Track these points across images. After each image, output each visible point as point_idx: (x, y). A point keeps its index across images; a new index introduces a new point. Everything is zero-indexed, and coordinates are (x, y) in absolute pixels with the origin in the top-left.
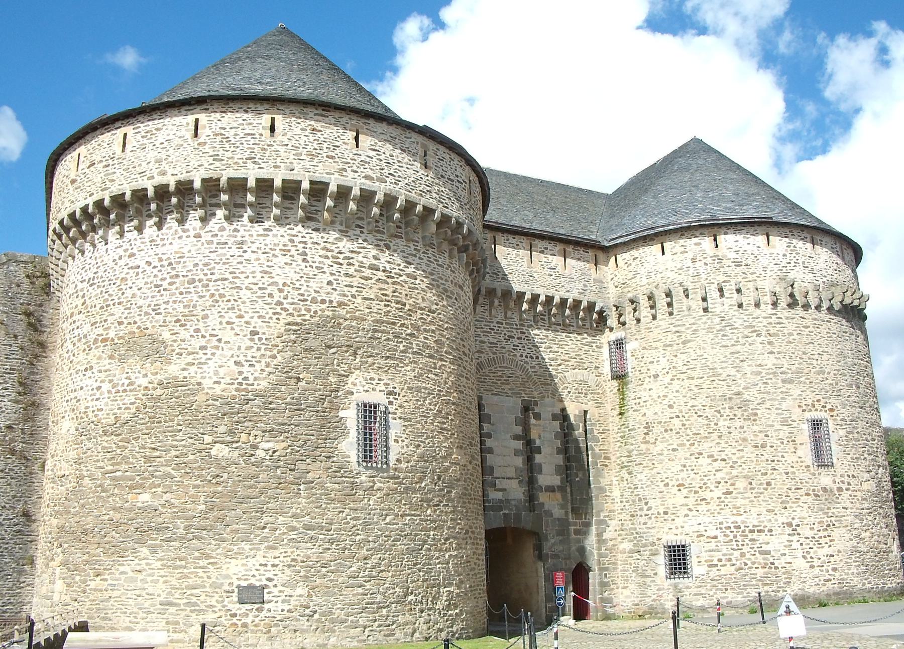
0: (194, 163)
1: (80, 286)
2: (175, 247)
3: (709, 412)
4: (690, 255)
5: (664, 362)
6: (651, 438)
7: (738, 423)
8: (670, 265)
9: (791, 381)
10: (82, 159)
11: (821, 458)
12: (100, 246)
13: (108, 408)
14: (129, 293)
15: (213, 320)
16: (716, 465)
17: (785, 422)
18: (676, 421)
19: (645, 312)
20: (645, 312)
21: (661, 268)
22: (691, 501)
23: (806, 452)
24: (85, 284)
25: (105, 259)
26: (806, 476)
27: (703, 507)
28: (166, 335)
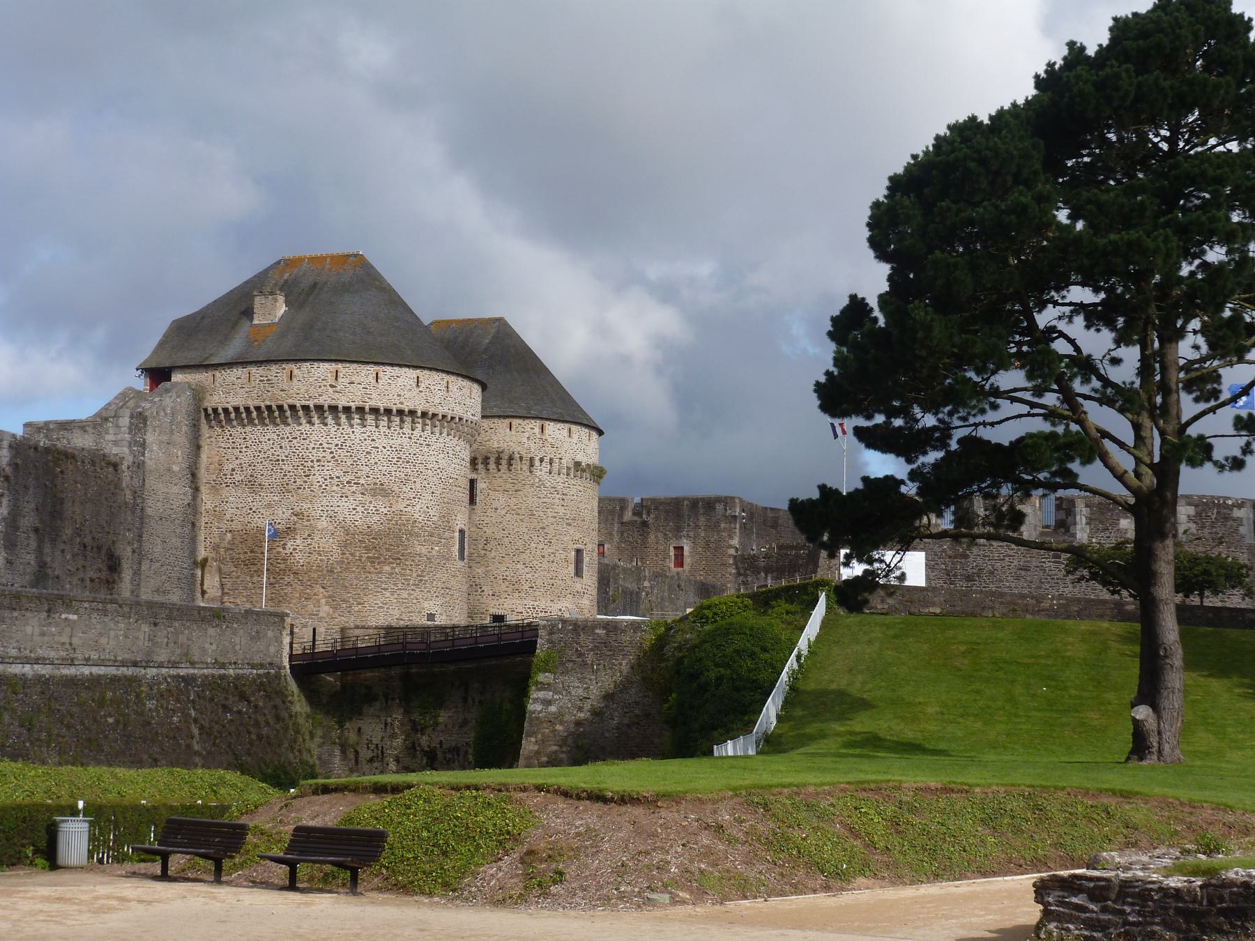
0: (417, 403)
1: (325, 445)
2: (399, 441)
3: (526, 538)
4: (527, 435)
5: (502, 501)
6: (488, 547)
7: (541, 546)
8: (514, 439)
9: (569, 524)
10: (340, 375)
11: (578, 572)
12: (358, 429)
13: (359, 519)
14: (372, 461)
15: (418, 485)
16: (527, 570)
17: (564, 549)
18: (506, 540)
19: (492, 466)
20: (492, 466)
21: (507, 439)
22: (510, 590)
23: (572, 568)
24: (333, 446)
25: (353, 437)
26: (570, 583)
27: (516, 595)
28: (395, 488)
